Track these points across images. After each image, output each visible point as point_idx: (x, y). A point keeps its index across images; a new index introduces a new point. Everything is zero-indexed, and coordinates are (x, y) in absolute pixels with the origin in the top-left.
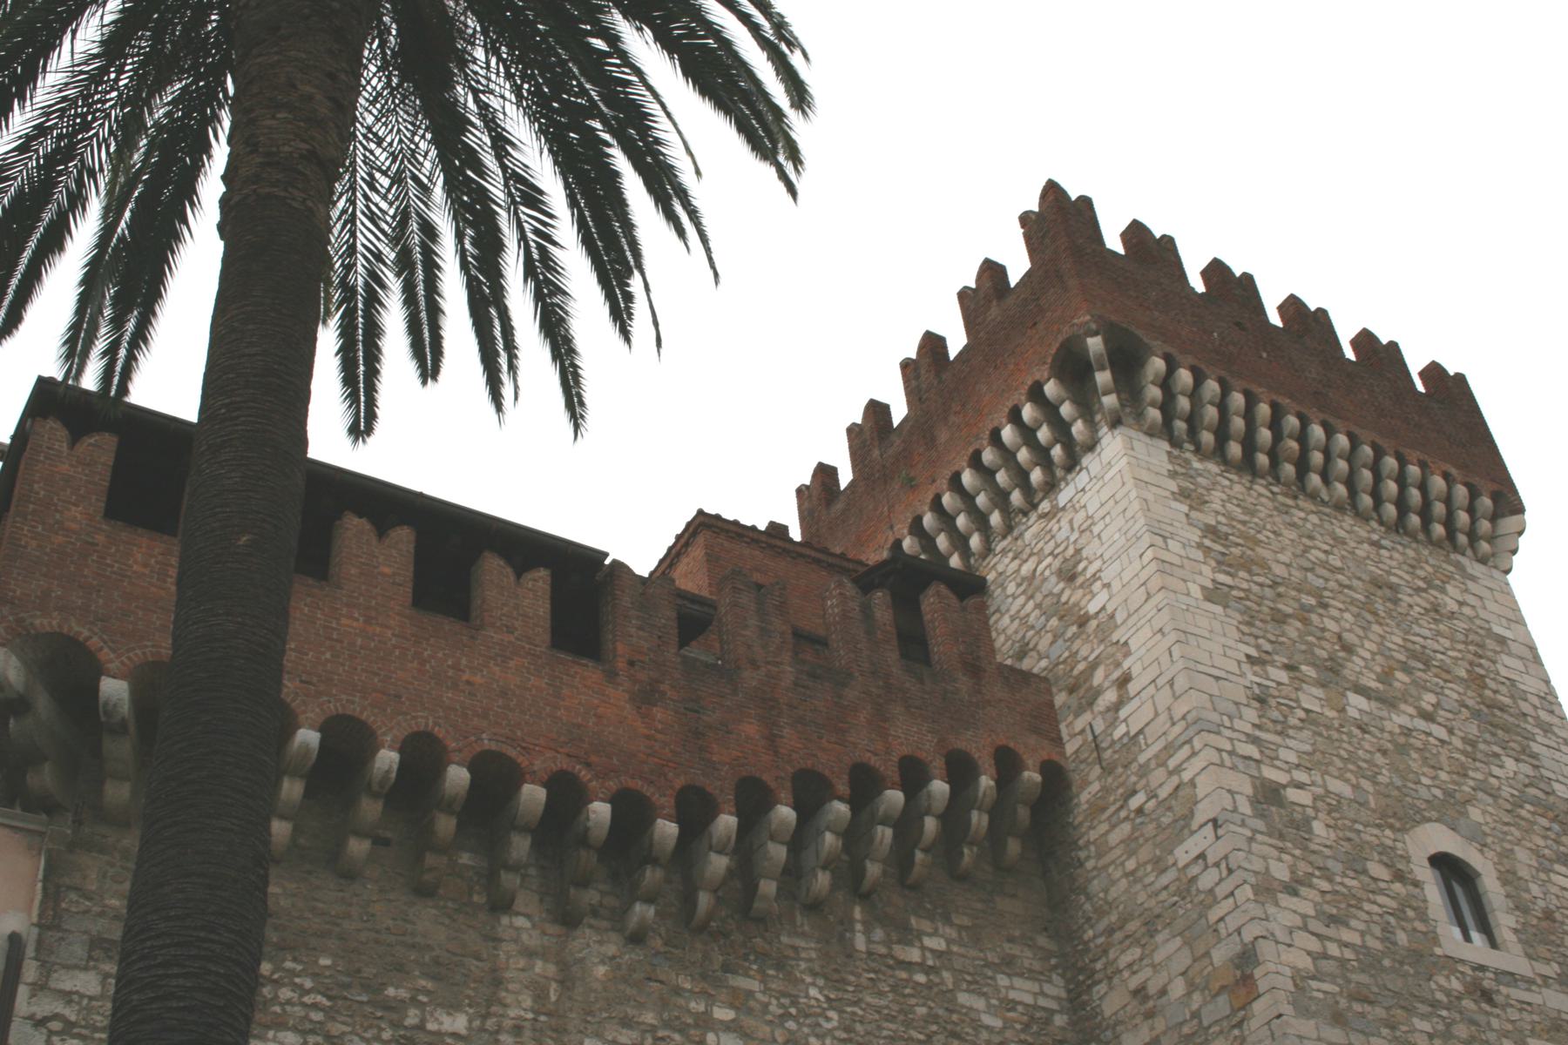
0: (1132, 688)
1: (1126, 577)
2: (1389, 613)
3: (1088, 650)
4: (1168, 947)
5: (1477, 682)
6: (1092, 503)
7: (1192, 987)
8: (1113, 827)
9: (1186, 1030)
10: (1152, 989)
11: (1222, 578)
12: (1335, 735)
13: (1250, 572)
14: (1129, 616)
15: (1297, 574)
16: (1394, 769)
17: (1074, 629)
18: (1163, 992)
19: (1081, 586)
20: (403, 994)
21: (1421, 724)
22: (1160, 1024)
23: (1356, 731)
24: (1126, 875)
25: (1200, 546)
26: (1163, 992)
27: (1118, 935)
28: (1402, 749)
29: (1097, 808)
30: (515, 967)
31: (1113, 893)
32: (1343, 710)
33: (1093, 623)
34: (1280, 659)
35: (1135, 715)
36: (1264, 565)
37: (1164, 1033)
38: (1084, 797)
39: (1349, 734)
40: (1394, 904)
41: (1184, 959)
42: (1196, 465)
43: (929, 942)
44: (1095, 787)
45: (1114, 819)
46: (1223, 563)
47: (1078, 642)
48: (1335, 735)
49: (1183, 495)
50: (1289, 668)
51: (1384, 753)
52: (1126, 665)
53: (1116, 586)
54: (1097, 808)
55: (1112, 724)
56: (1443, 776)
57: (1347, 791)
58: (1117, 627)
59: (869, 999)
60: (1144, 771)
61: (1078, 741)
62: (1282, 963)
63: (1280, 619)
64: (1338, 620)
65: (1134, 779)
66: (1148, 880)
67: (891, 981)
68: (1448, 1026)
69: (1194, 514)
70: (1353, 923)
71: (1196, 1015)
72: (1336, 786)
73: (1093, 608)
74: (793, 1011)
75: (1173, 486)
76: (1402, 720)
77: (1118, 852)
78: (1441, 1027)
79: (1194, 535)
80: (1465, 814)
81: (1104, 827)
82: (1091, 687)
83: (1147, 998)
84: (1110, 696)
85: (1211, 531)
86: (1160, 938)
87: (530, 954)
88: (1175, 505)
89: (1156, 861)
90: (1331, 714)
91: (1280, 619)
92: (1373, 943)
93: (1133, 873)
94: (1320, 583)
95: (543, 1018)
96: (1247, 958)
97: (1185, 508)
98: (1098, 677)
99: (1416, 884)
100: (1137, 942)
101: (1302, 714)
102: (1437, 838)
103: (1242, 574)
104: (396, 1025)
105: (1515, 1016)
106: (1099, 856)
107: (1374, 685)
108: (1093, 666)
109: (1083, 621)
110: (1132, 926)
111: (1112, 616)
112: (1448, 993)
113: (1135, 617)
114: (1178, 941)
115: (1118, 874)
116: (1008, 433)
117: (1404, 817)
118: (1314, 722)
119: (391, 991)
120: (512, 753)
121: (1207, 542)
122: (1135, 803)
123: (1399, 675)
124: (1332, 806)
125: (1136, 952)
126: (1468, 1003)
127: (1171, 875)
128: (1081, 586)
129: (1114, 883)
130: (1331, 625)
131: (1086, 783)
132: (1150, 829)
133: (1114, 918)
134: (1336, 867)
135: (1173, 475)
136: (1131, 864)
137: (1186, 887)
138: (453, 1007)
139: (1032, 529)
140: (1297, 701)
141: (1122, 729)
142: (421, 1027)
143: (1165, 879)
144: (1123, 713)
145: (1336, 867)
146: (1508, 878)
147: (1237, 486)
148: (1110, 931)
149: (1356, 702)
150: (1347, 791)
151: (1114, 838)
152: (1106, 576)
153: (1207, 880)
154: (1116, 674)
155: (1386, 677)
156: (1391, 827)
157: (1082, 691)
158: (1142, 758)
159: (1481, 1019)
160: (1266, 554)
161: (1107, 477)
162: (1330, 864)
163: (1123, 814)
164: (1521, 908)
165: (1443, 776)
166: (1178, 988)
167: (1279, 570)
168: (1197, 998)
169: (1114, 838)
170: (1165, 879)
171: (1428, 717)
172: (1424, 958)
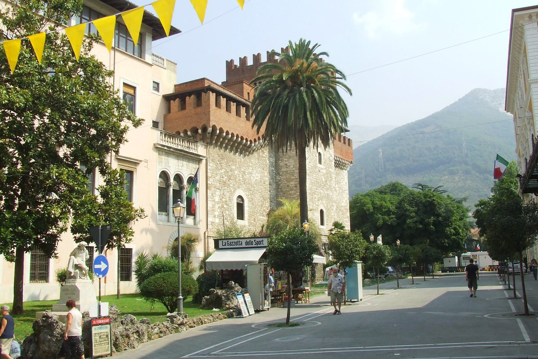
7: (294, 167)
22: (288, 169)
41: (294, 163)
166: (292, 166)
172: (316, 167)
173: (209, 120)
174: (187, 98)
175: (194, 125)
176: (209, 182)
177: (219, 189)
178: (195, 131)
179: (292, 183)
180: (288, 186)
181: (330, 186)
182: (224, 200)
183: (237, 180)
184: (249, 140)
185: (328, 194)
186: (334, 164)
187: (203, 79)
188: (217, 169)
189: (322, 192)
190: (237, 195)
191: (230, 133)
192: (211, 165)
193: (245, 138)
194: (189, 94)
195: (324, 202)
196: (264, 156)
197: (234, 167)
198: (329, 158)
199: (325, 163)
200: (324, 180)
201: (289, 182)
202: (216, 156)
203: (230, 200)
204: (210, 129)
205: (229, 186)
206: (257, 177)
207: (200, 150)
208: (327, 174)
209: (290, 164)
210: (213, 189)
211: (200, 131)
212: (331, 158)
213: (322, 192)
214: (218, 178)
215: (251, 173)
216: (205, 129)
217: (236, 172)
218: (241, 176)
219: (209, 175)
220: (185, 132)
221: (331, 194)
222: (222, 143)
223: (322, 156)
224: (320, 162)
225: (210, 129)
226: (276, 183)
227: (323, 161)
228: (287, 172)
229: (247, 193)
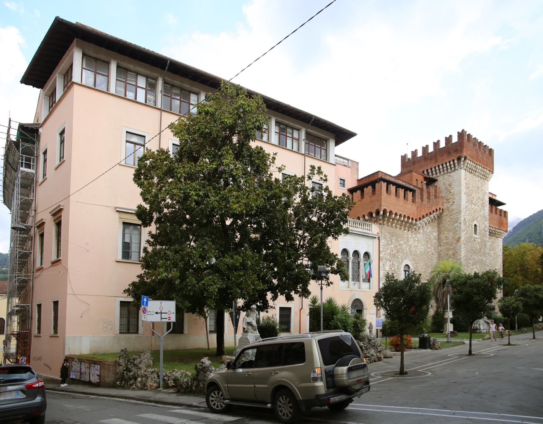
3: (450, 197)
4: (451, 233)
5: (483, 200)
29: (446, 215)
35: (454, 207)
54: (446, 215)
60: (453, 214)
62: (462, 239)
84: (451, 203)
96: (460, 238)
98: (450, 200)
102: (475, 223)
109: (450, 192)
116: (448, 164)
117: (473, 221)
124: (469, 220)
137: (455, 228)
139: (446, 176)
146: (479, 227)
149: (473, 205)
153: (457, 229)
166: (451, 238)
172: (471, 237)
173: (381, 206)
174: (365, 189)
175: (369, 211)
176: (381, 255)
177: (389, 260)
178: (371, 214)
179: (450, 252)
180: (447, 254)
181: (484, 253)
182: (393, 269)
183: (405, 252)
184: (414, 219)
185: (482, 260)
186: (488, 233)
187: (378, 172)
188: (388, 244)
189: (476, 258)
190: (404, 264)
191: (398, 214)
192: (383, 241)
193: (411, 217)
194: (366, 185)
197: (402, 242)
198: (484, 229)
199: (480, 233)
201: (448, 251)
202: (387, 234)
203: (399, 268)
204: (382, 213)
205: (397, 258)
206: (421, 249)
207: (375, 229)
208: (482, 242)
210: (384, 260)
211: (374, 215)
212: (486, 229)
213: (476, 258)
214: (388, 251)
215: (417, 246)
216: (378, 213)
217: (404, 246)
218: (408, 249)
219: (381, 249)
220: (364, 216)
221: (484, 259)
222: (392, 223)
223: (478, 228)
225: (382, 213)
226: (438, 252)
227: (478, 231)
228: (447, 243)
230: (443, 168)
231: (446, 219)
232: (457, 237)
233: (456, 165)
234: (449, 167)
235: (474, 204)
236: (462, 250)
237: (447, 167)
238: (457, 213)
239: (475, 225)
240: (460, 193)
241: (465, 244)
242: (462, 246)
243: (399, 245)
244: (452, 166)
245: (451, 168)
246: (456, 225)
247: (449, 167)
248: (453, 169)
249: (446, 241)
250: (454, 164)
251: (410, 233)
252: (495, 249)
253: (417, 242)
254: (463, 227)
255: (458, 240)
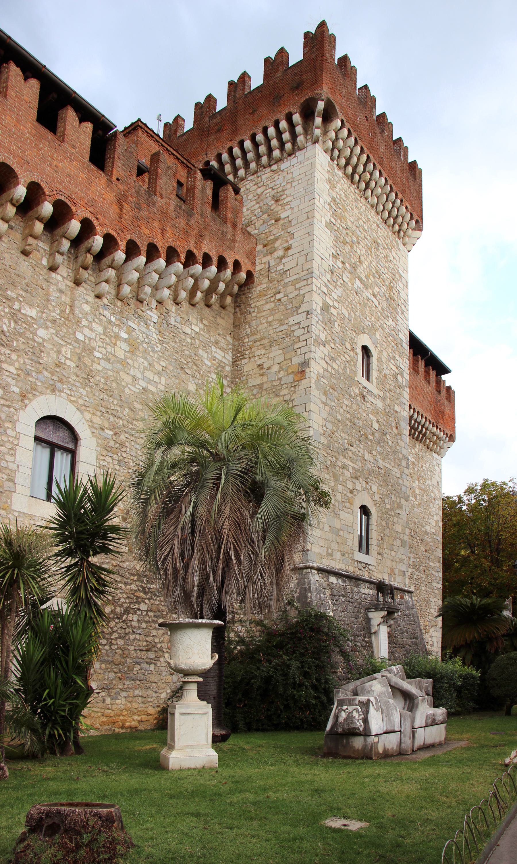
0: (290, 252)
1: (301, 207)
2: (375, 253)
3: (276, 232)
4: (276, 352)
6: (296, 172)
7: (281, 369)
8: (267, 303)
9: (274, 383)
10: (265, 366)
11: (333, 220)
12: (349, 293)
13: (341, 221)
14: (297, 224)
15: (354, 228)
16: (361, 312)
17: (273, 221)
18: (269, 368)
19: (281, 205)
20: (14, 295)
21: (372, 298)
22: (265, 379)
23: (355, 294)
24: (267, 322)
25: (329, 204)
26: (269, 368)
27: (258, 343)
28: (365, 305)
29: (262, 295)
30: (54, 294)
31: (260, 328)
32: (353, 285)
33: (281, 222)
34: (341, 259)
36: (345, 219)
37: (266, 382)
38: (258, 288)
39: (353, 294)
40: (349, 359)
41: (281, 359)
42: (336, 171)
43: (194, 327)
44: (264, 286)
45: (268, 300)
46: (335, 215)
47: (273, 227)
48: (349, 293)
49: (329, 181)
50: (343, 263)
51: (360, 304)
52: (290, 242)
53: (295, 210)
54: (262, 295)
55: (278, 264)
56: (373, 319)
57: (347, 315)
58: (291, 226)
59: (171, 343)
60: (286, 285)
61: (262, 266)
63: (345, 243)
64: (361, 250)
65: (280, 287)
66: (275, 327)
67: (180, 338)
68: (352, 404)
69: (330, 190)
70: (337, 362)
71: (280, 379)
72: (345, 312)
73: (283, 216)
74: (146, 340)
75: (327, 176)
76: (368, 294)
77: (266, 313)
78: (350, 404)
79: (329, 200)
80: (374, 334)
81: (264, 302)
82: (274, 247)
83: (262, 368)
84: (280, 253)
85: (334, 200)
86: (273, 349)
87: (61, 292)
88: (326, 184)
89: (281, 320)
90: (350, 285)
91: (345, 243)
92: (341, 371)
93: (270, 322)
94: (359, 233)
95: (63, 319)
97: (329, 188)
98: (277, 244)
99: (356, 354)
100: (265, 348)
101: (342, 282)
102: (365, 340)
103: (338, 221)
104: (10, 307)
105: (368, 406)
106: (258, 312)
107: (364, 278)
108: (276, 239)
110: (263, 342)
111: (290, 222)
112: (355, 393)
113: (299, 225)
114: (281, 352)
115: (264, 321)
117: (359, 330)
118: (344, 286)
119: (9, 292)
120: (69, 203)
121: (332, 204)
122: (278, 296)
123: (371, 277)
125: (263, 351)
126: (358, 398)
127: (285, 327)
128: (281, 205)
129: (261, 324)
130: (358, 251)
131: (260, 283)
132: (282, 308)
133: (258, 337)
134: (338, 341)
135: (328, 172)
136: (270, 319)
138: (31, 306)
140: (342, 276)
141: (281, 267)
142: (19, 311)
143: (282, 328)
144: (283, 261)
145: (338, 341)
146: (379, 360)
147: (345, 183)
148: (255, 341)
149: (358, 282)
150: (347, 315)
151: (267, 307)
152: (293, 204)
154: (286, 245)
155: (367, 277)
156: (355, 332)
157: (269, 248)
158: (286, 281)
159: (360, 404)
160: (347, 215)
161: (305, 164)
162: (336, 339)
163: (272, 299)
164: (379, 371)
165: (373, 319)
166: (276, 368)
167: (350, 224)
168: (282, 374)
169: (267, 307)
170: (282, 328)
171: (375, 296)
185: (387, 470)
195: (375, 488)
196: (188, 331)
198: (395, 376)
200: (376, 426)
209: (270, 363)
212: (399, 377)
215: (124, 363)
223: (374, 360)
224: (367, 372)
227: (374, 374)
228: (260, 386)
229: (97, 420)
230: (256, 145)
231: (261, 302)
232: (296, 360)
233: (299, 129)
234: (274, 143)
235: (360, 279)
236: (312, 407)
237: (268, 140)
238: (298, 280)
239: (365, 349)
240: (310, 216)
241: (325, 393)
242: (315, 392)
243: (14, 316)
244: (286, 136)
245: (282, 145)
246: (293, 320)
247: (274, 143)
248: (288, 146)
249: (258, 381)
250: (292, 126)
251: (84, 293)
252: (425, 480)
253: (125, 346)
254: (318, 331)
255: (301, 372)
